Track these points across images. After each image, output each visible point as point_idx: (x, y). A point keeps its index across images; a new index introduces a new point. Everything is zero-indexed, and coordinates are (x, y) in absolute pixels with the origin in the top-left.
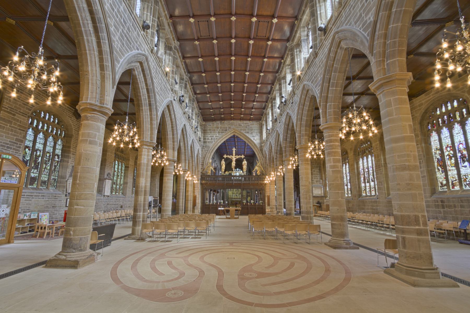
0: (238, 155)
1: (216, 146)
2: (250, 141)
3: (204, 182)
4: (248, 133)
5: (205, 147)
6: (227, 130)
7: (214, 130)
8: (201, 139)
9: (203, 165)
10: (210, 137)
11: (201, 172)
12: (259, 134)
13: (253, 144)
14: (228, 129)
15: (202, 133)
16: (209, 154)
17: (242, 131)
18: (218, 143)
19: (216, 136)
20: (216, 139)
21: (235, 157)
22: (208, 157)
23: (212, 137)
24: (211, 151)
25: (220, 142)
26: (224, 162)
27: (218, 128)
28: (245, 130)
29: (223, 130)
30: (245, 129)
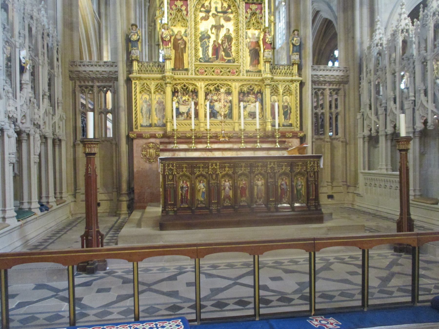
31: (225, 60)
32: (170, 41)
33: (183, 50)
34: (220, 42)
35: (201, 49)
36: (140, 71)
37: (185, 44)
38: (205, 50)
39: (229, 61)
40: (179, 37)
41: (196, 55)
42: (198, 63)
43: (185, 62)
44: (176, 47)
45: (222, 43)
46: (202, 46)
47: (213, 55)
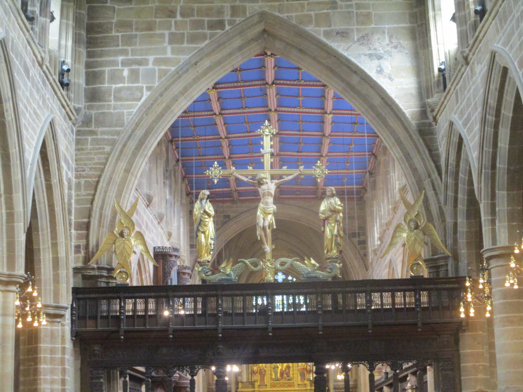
0: (293, 164)
1: (161, 115)
2: (355, 80)
3: (90, 327)
4: (343, 35)
5: (100, 123)
6: (220, 24)
7: (150, 27)
8: (72, 78)
9: (87, 226)
10: (124, 64)
11: (76, 270)
12: (406, 43)
13: (377, 101)
14: (227, 17)
15: (77, 41)
16: (122, 165)
17: (310, 29)
18: (175, 99)
19: (157, 62)
20: (163, 73)
21: (273, 177)
22: (118, 178)
23: (140, 63)
24: (132, 144)
25: (186, 89)
26: (209, 208)
27: (172, 14)
28: (327, 20)
29: (198, 24)
30: (327, 15)
31: (286, 379)
32: (257, 372)
33: (264, 375)
34: (284, 369)
35: (273, 374)
36: (242, 387)
37: (265, 371)
38: (276, 374)
39: (289, 380)
40: (262, 368)
41: (271, 378)
42: (272, 382)
43: (265, 381)
44: (261, 373)
45: (285, 370)
46: (274, 372)
47: (280, 376)
